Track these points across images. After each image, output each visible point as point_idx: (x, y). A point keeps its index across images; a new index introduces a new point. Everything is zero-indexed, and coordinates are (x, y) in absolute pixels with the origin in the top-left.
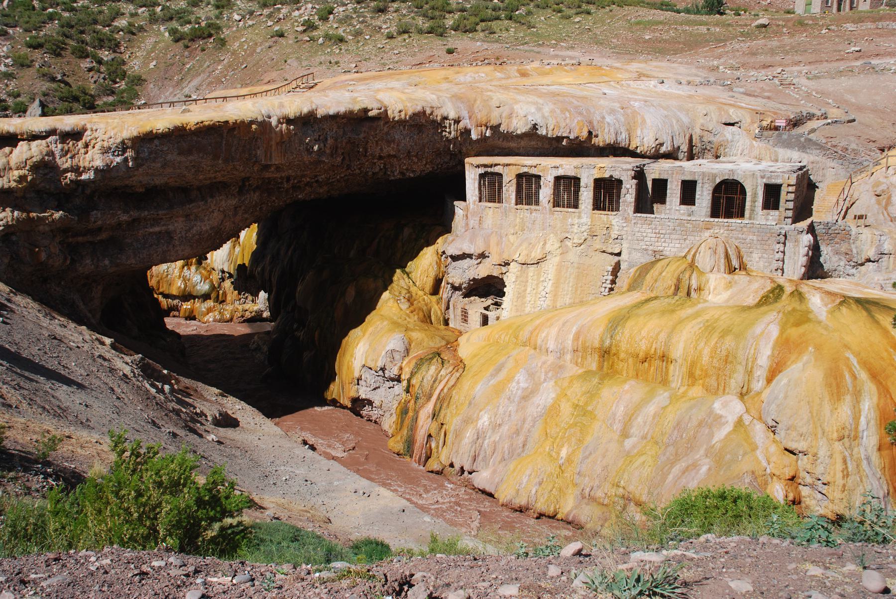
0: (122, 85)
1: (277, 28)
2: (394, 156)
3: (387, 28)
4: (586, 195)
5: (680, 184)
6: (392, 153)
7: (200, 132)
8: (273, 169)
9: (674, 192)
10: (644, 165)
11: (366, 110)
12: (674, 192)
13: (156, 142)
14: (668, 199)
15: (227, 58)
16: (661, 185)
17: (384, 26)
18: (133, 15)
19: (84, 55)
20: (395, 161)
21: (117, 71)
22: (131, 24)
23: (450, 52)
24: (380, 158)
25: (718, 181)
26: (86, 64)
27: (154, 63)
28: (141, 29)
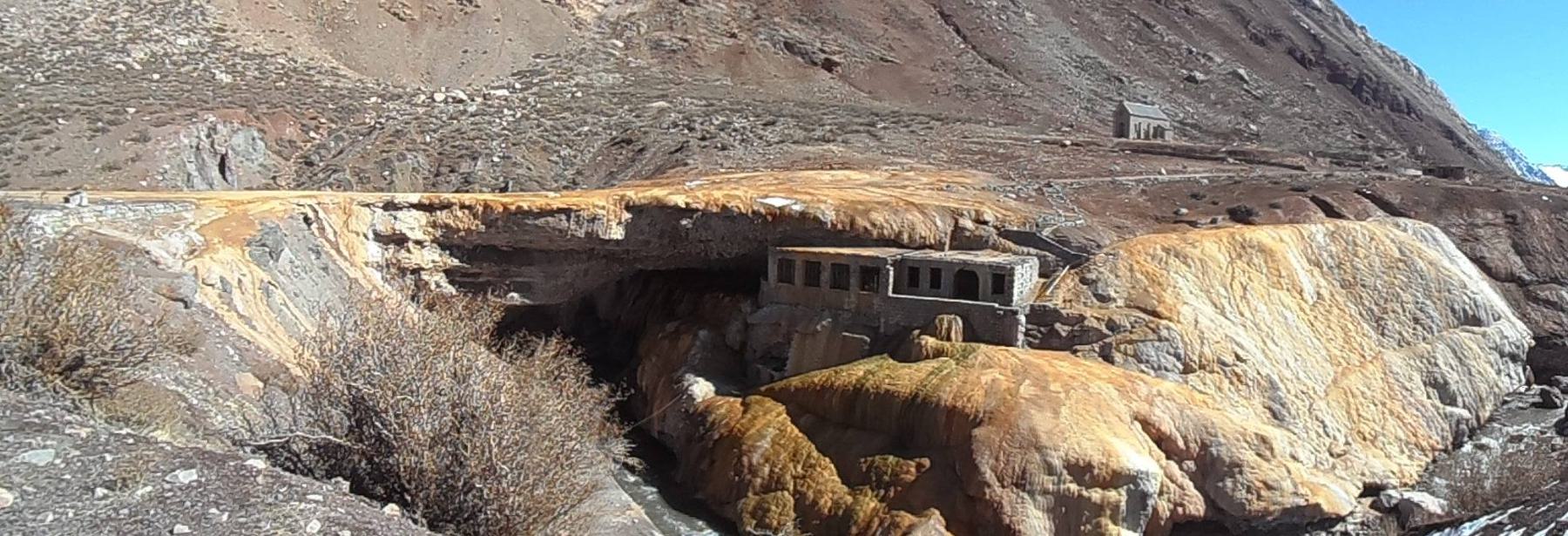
9: (925, 279)
12: (925, 279)
14: (920, 283)
20: (712, 243)
22: (590, 131)
24: (701, 241)
25: (957, 269)
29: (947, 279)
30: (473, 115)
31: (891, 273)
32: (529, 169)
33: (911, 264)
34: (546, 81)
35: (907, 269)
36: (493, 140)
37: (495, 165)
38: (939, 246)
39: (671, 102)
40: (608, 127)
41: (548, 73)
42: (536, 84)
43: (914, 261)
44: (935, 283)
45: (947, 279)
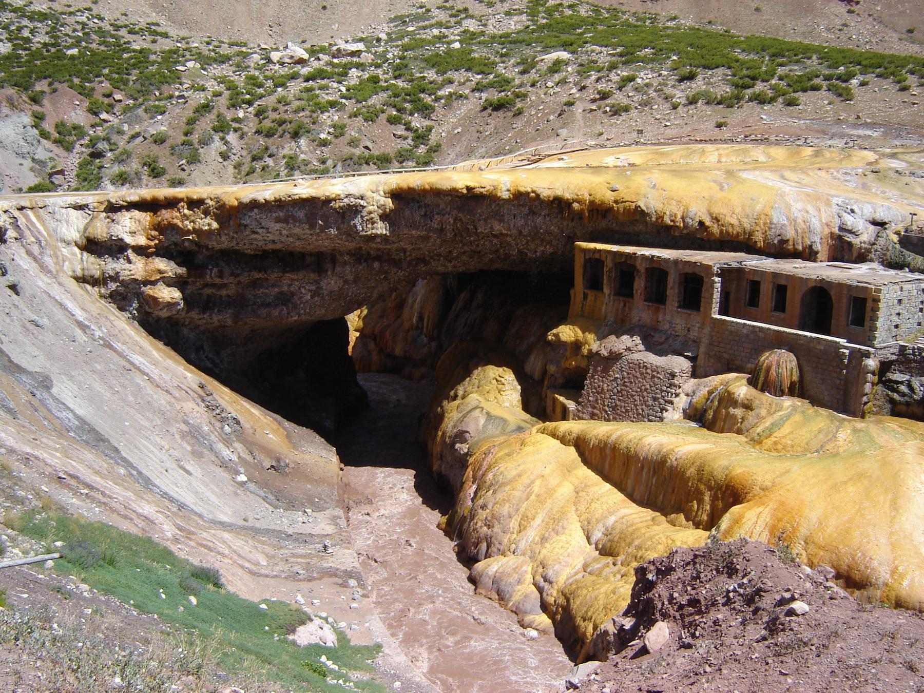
0: (422, 150)
1: (577, 95)
2: (507, 235)
3: (680, 98)
4: (673, 291)
5: (771, 288)
6: (504, 232)
7: (296, 203)
8: (379, 240)
10: (740, 263)
11: (469, 189)
12: (767, 293)
13: (256, 211)
15: (519, 124)
16: (755, 286)
17: (678, 96)
18: (461, 84)
19: (392, 121)
21: (421, 137)
23: (719, 126)
24: (495, 236)
26: (400, 130)
27: (459, 130)
28: (461, 96)
29: (794, 300)
30: (307, 80)
31: (718, 286)
32: (366, 148)
33: (751, 278)
34: (424, 28)
35: (745, 284)
36: (322, 113)
37: (324, 143)
38: (809, 254)
39: (573, 53)
40: (478, 88)
41: (433, 18)
42: (408, 34)
43: (754, 272)
44: (780, 304)
45: (794, 300)
